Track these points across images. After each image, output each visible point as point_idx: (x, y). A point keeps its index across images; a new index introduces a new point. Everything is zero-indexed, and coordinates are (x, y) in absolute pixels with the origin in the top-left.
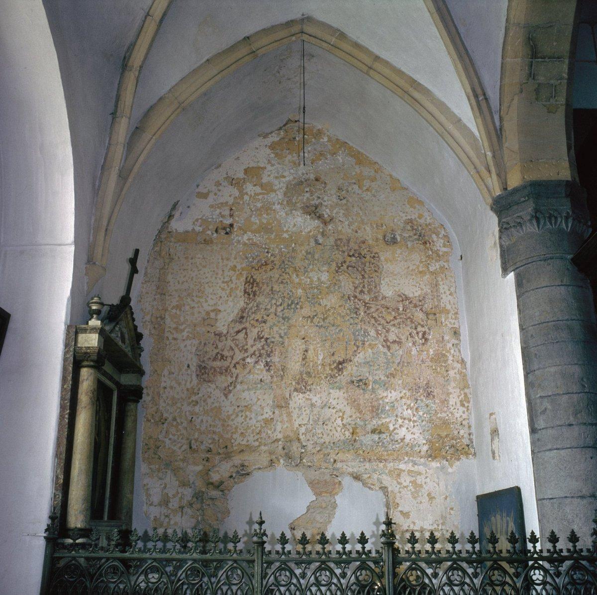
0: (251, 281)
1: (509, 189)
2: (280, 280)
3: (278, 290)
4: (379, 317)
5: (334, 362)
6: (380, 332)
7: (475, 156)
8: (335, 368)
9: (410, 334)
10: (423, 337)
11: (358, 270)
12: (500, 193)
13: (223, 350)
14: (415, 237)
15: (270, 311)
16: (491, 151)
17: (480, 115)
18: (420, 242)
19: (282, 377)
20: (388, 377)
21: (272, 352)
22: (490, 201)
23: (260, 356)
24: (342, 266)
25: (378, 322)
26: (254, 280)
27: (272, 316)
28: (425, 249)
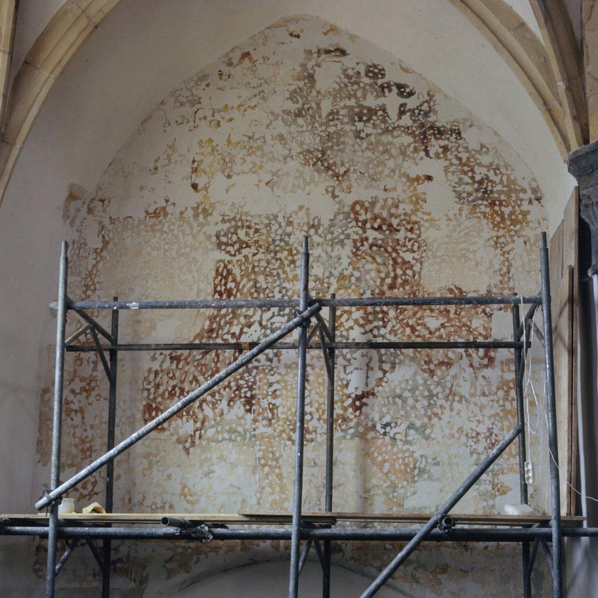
0: (225, 274)
1: (592, 142)
2: (268, 270)
3: (264, 286)
4: (418, 325)
5: (349, 396)
7: (545, 84)
8: (350, 406)
11: (386, 250)
12: (578, 148)
13: (182, 382)
14: (480, 195)
15: (252, 320)
16: (563, 80)
17: (546, 22)
18: (485, 203)
19: (270, 420)
20: (430, 419)
21: (254, 383)
22: (567, 157)
23: (237, 390)
24: (363, 245)
25: (417, 333)
26: (229, 272)
27: (256, 326)
28: (492, 215)
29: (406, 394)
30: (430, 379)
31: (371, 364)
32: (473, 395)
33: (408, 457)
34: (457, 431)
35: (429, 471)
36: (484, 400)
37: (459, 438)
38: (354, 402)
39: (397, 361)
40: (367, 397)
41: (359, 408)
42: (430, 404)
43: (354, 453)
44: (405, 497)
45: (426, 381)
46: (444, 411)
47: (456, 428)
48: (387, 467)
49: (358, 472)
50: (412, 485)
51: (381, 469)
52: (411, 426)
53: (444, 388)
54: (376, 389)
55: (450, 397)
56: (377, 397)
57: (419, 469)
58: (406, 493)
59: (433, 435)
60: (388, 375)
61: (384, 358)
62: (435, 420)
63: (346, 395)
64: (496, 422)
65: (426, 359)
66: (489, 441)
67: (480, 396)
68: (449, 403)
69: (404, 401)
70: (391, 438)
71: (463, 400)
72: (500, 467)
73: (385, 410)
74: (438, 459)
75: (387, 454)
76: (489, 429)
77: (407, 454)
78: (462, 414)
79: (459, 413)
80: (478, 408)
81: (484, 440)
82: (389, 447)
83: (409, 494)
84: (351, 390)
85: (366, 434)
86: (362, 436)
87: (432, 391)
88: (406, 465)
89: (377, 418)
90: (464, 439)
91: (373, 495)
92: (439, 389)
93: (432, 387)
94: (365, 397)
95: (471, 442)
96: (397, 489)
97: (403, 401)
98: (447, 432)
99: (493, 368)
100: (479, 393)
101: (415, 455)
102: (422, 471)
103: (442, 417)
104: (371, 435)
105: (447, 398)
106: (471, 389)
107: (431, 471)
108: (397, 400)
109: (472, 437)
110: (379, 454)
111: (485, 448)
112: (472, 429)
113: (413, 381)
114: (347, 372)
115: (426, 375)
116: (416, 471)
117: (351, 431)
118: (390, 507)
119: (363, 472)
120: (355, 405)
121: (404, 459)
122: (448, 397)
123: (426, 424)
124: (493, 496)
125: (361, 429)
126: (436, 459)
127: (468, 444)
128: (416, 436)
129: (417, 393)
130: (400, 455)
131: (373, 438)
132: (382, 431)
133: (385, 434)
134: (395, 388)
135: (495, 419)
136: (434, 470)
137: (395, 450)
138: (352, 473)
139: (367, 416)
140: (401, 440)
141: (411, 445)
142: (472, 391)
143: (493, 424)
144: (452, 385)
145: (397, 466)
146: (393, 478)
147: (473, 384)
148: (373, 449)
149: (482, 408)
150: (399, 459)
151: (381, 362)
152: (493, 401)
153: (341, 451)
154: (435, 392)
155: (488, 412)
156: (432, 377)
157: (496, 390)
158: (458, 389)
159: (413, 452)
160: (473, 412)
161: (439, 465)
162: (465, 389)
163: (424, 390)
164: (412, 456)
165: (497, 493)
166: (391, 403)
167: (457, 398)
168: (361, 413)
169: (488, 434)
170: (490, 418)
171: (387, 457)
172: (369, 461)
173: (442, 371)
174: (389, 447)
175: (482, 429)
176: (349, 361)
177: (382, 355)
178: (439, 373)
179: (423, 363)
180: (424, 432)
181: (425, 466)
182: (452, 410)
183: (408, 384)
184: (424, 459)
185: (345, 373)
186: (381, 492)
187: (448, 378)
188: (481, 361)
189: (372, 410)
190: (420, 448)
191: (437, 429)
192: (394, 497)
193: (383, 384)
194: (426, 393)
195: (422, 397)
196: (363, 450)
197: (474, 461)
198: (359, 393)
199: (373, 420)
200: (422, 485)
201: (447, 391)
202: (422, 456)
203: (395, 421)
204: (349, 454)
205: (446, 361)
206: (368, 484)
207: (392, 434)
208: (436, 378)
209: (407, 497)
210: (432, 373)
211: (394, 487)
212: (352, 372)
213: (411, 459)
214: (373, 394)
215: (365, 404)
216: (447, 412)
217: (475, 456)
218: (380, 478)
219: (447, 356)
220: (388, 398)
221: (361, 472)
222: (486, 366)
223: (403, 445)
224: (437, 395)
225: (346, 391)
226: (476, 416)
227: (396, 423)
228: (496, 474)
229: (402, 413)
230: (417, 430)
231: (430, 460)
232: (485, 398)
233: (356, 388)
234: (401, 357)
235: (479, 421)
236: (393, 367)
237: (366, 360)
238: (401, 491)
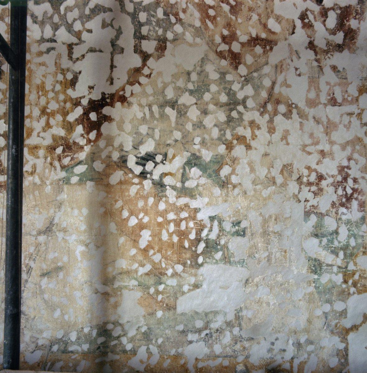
5: (77, 103)
6: (212, 12)
8: (79, 121)
9: (303, 17)
10: (341, 25)
20: (230, 147)
29: (186, 99)
30: (231, 70)
31: (120, 43)
32: (312, 103)
33: (185, 219)
34: (282, 172)
35: (225, 247)
36: (333, 113)
37: (284, 185)
38: (86, 113)
39: (170, 35)
40: (112, 105)
41: (96, 126)
42: (230, 120)
43: (85, 211)
44: (178, 292)
45: (223, 74)
46: (257, 132)
47: (278, 165)
48: (146, 236)
49: (92, 246)
50: (193, 271)
51: (135, 242)
52: (194, 161)
53: (257, 88)
54: (128, 88)
55: (269, 107)
56: (130, 104)
57: (207, 241)
58: (180, 286)
59: (234, 179)
60: (151, 62)
61: (145, 30)
62: (239, 150)
63: (71, 99)
64: (356, 156)
65: (226, 32)
66: (340, 192)
67: (325, 105)
68: (267, 117)
69: (182, 112)
70: (154, 183)
71: (295, 111)
72: (360, 241)
73: (144, 129)
74: (243, 225)
75: (146, 213)
76: (341, 169)
77: (184, 215)
78: (290, 139)
79: (284, 138)
80: (321, 128)
81: (331, 189)
82: (151, 200)
83: (186, 288)
84: (81, 90)
85: (108, 176)
86: (100, 179)
87: (235, 94)
88: (183, 235)
89: (128, 146)
90: (293, 187)
91: (120, 289)
92: (249, 90)
93: (236, 87)
94: (107, 104)
95: (306, 193)
96: (164, 279)
97: (179, 112)
98: (262, 172)
99: (353, 51)
100: (324, 98)
101: (200, 216)
102: (212, 247)
103: (253, 144)
104: (117, 176)
105: (263, 108)
106: (309, 91)
107: (230, 246)
108: (168, 110)
109: (310, 184)
110: (132, 213)
111: (333, 204)
112: (308, 168)
113: (199, 74)
114: (75, 56)
115: (224, 63)
116: (202, 246)
117: (81, 169)
118: (150, 311)
119: (102, 245)
120: (89, 119)
121: (177, 223)
122: (264, 106)
123: (222, 157)
124: (344, 295)
125: (99, 166)
126: (239, 223)
127: (302, 197)
128: (203, 181)
129: (207, 97)
130: (171, 216)
131: (121, 183)
132: (138, 170)
133: (143, 175)
134: (164, 88)
135: (353, 151)
136: (236, 245)
137: (162, 206)
138: (80, 249)
139: (110, 141)
140: (174, 188)
141: (192, 197)
142: (312, 95)
143: (349, 159)
144: (274, 83)
145: (165, 236)
146: (157, 258)
147: (313, 82)
148: (119, 204)
149: (330, 127)
150: (169, 222)
151: (139, 37)
152: (350, 114)
153: (60, 207)
154: (240, 96)
155: (341, 135)
156: (236, 68)
157: (356, 94)
158: (285, 91)
159: (196, 210)
160: (311, 135)
161: (244, 235)
162: (297, 91)
163: (219, 93)
164: (194, 218)
165: (352, 290)
166: (157, 115)
167: (282, 108)
168: (99, 135)
169: (339, 178)
170: (343, 148)
171: (146, 220)
172: (113, 227)
173: (254, 56)
174: (151, 200)
175: (330, 168)
176: (78, 35)
177: (141, 25)
178: (249, 59)
179: (218, 39)
180: (217, 172)
181: (219, 236)
182: (272, 130)
183: (189, 80)
184: (216, 223)
185: (70, 58)
186: (136, 283)
187: (267, 70)
188: (331, 38)
189: (121, 128)
190: (208, 205)
191: (243, 168)
192: (158, 292)
193: (142, 80)
194: (224, 98)
195: (216, 104)
196: (103, 204)
197: (312, 229)
198: (96, 96)
199: (121, 148)
200: (210, 271)
201: (264, 94)
202: (212, 219)
203: (163, 151)
204: (76, 212)
205: (263, 36)
206: (110, 269)
207: (156, 177)
208: (242, 70)
209: (183, 293)
210: (236, 59)
211: (158, 274)
212: (83, 56)
213: (191, 224)
214: (123, 99)
215: (108, 119)
216: (263, 134)
217: (313, 219)
218: (133, 259)
219: (265, 26)
220: (150, 106)
221: (98, 247)
222: (340, 48)
223: (178, 197)
224: (244, 102)
225: (72, 94)
226: (317, 143)
227: (165, 155)
228: (352, 255)
229: (178, 135)
230: (204, 168)
231: (228, 226)
232: (336, 108)
233: (91, 88)
234: (178, 28)
235: (322, 153)
236: (162, 47)
237: (110, 33)
238: (172, 282)
